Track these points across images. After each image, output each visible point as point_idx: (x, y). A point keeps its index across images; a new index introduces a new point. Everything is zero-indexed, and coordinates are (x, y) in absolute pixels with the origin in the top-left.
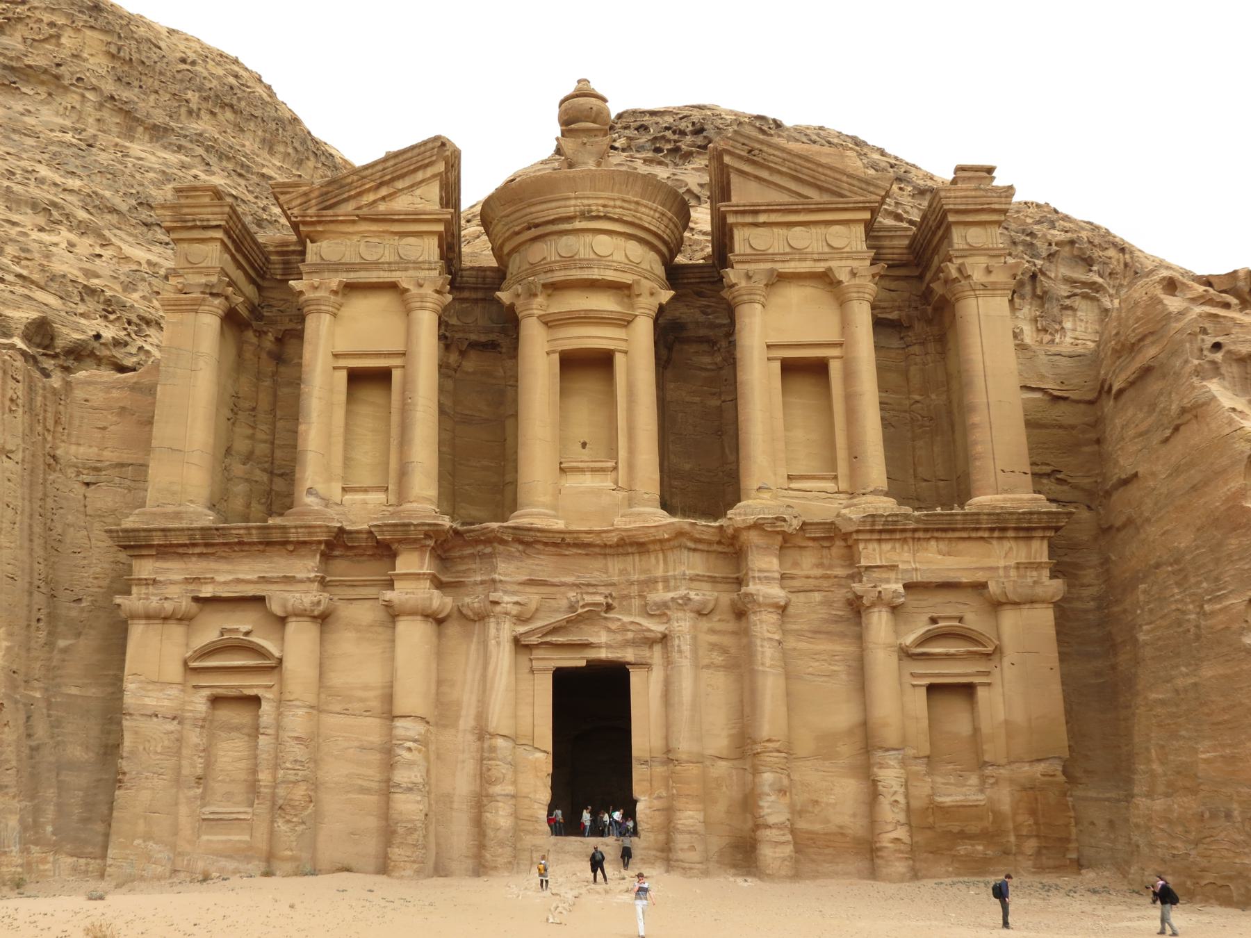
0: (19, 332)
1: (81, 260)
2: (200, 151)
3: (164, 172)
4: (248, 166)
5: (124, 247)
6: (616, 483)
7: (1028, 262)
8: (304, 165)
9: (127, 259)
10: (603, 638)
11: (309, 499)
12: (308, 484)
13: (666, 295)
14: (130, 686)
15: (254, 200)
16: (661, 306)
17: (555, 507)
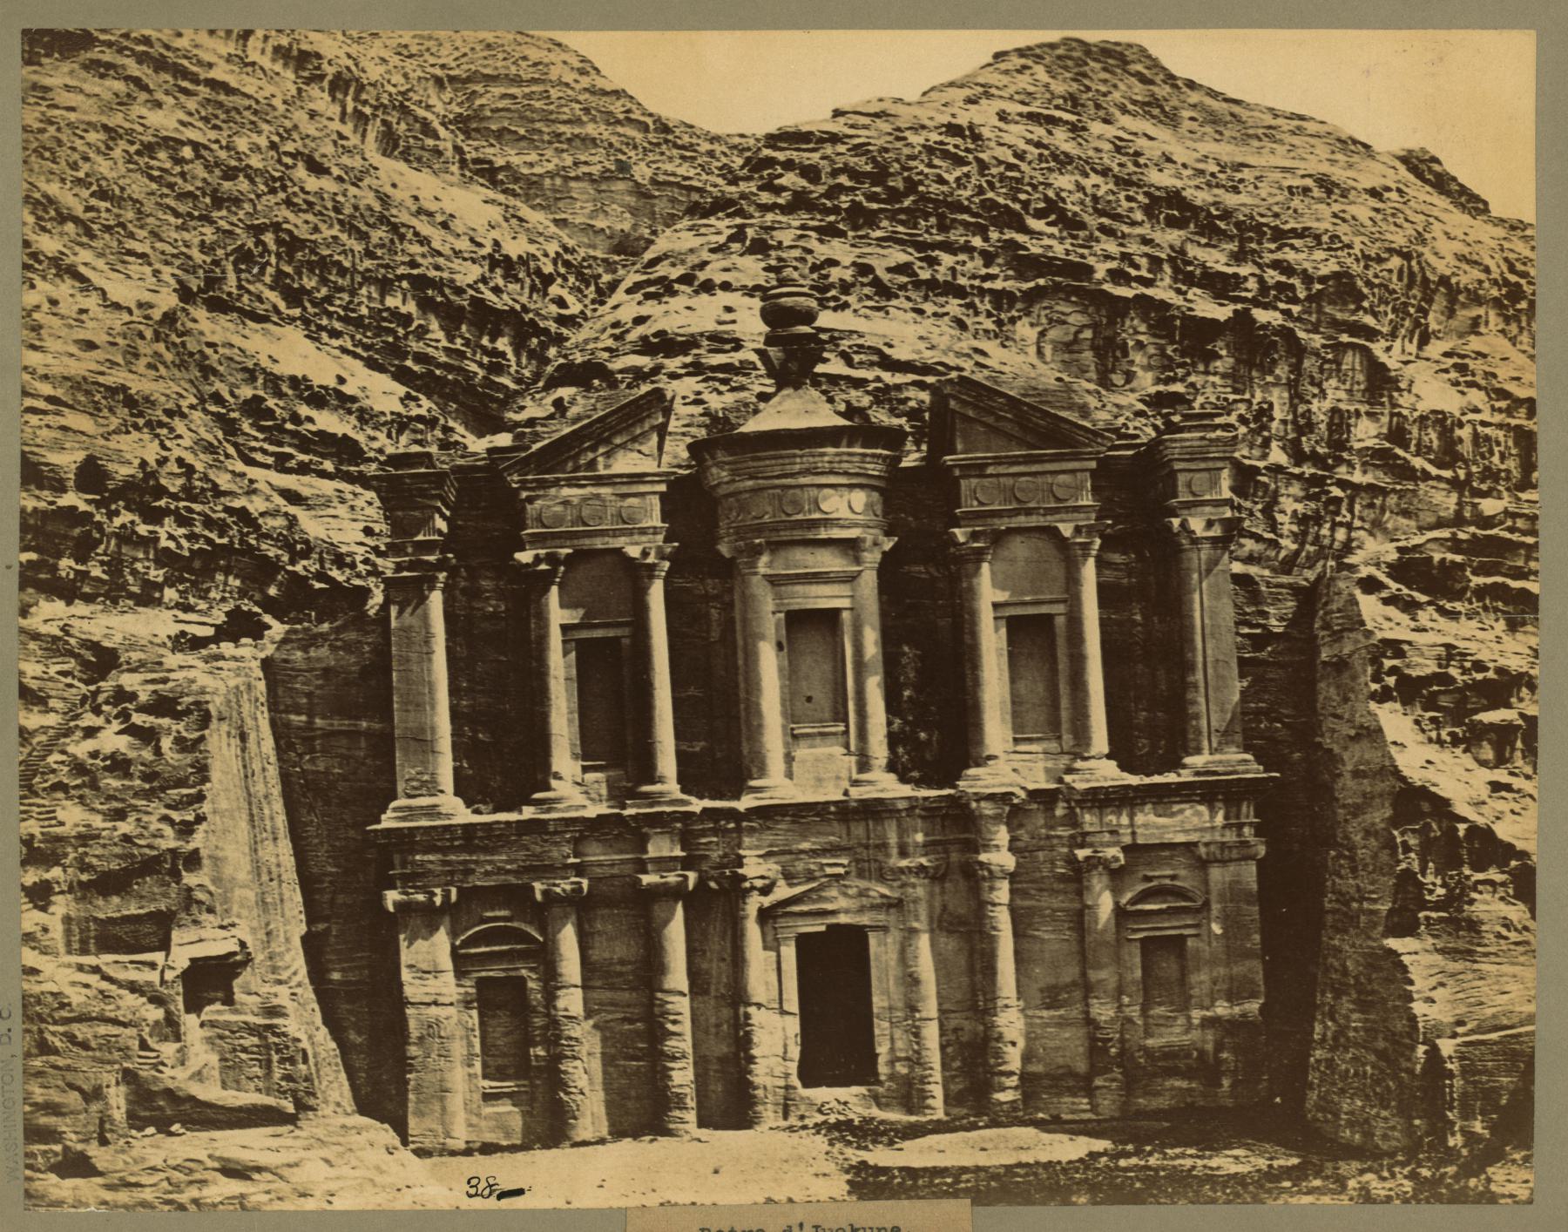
0: (71, 483)
1: (71, 327)
2: (133, 68)
3: (106, 128)
4: (193, 74)
5: (107, 286)
6: (847, 746)
7: (1283, 312)
8: (252, 39)
9: (117, 306)
10: (843, 903)
11: (554, 783)
12: (555, 768)
13: (888, 544)
14: (406, 975)
15: (213, 135)
16: (884, 553)
17: (789, 775)
